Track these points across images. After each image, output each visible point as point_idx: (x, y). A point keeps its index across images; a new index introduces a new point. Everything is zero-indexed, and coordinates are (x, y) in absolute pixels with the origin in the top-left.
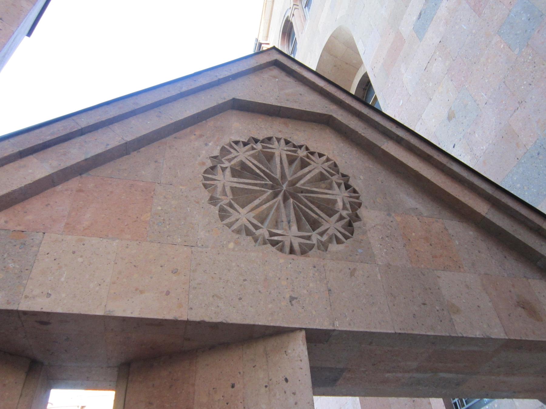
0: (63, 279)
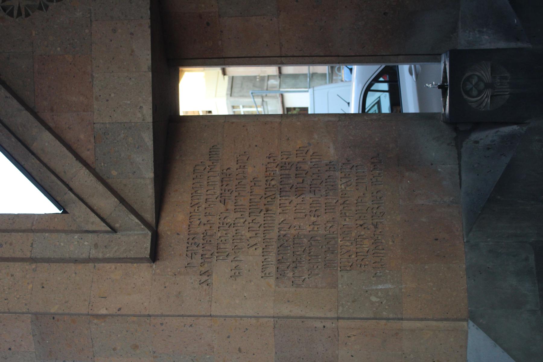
0: (129, 102)
